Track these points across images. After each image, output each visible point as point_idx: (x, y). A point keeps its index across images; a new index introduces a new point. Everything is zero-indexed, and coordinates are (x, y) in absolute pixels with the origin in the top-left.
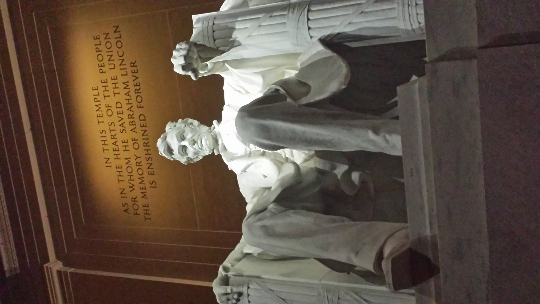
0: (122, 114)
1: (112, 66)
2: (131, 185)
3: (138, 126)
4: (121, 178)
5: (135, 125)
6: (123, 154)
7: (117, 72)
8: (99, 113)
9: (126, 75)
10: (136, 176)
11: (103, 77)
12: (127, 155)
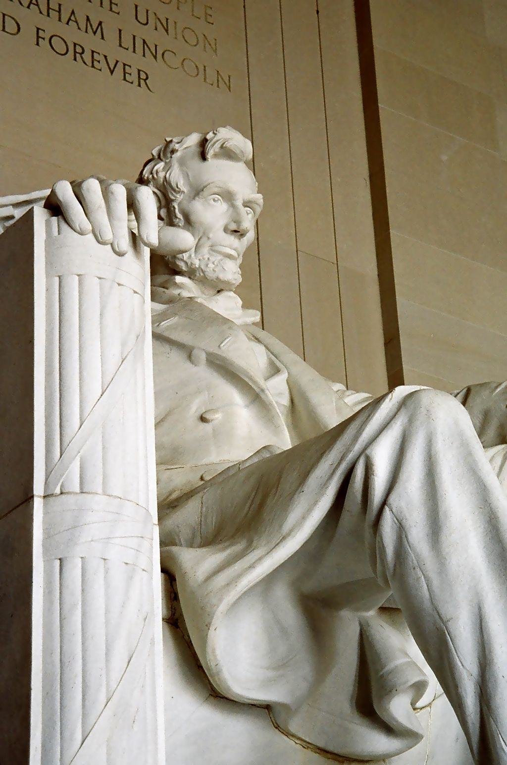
1: (142, 18)
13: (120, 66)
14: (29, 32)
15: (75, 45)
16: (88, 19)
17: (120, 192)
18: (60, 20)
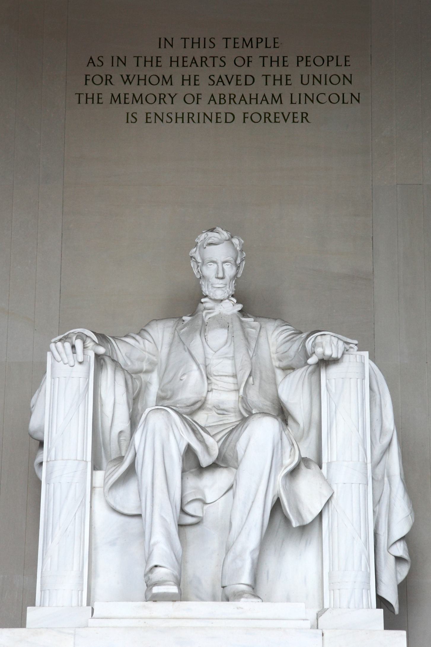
0: (237, 84)
1: (305, 82)
2: (131, 78)
4: (142, 61)
5: (220, 103)
6: (177, 73)
7: (297, 88)
8: (240, 41)
9: (292, 103)
11: (292, 60)
12: (177, 80)
13: (291, 115)
14: (239, 117)
15: (265, 113)
16: (273, 95)
17: (68, 345)
18: (257, 103)
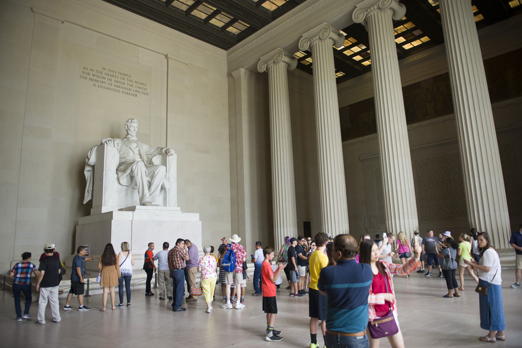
3: (116, 88)
6: (107, 77)
7: (135, 89)
10: (99, 79)
11: (134, 81)
12: (106, 79)
